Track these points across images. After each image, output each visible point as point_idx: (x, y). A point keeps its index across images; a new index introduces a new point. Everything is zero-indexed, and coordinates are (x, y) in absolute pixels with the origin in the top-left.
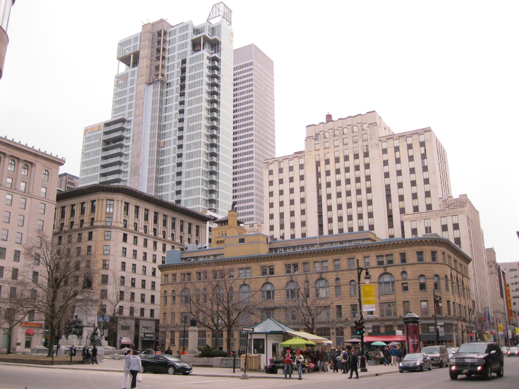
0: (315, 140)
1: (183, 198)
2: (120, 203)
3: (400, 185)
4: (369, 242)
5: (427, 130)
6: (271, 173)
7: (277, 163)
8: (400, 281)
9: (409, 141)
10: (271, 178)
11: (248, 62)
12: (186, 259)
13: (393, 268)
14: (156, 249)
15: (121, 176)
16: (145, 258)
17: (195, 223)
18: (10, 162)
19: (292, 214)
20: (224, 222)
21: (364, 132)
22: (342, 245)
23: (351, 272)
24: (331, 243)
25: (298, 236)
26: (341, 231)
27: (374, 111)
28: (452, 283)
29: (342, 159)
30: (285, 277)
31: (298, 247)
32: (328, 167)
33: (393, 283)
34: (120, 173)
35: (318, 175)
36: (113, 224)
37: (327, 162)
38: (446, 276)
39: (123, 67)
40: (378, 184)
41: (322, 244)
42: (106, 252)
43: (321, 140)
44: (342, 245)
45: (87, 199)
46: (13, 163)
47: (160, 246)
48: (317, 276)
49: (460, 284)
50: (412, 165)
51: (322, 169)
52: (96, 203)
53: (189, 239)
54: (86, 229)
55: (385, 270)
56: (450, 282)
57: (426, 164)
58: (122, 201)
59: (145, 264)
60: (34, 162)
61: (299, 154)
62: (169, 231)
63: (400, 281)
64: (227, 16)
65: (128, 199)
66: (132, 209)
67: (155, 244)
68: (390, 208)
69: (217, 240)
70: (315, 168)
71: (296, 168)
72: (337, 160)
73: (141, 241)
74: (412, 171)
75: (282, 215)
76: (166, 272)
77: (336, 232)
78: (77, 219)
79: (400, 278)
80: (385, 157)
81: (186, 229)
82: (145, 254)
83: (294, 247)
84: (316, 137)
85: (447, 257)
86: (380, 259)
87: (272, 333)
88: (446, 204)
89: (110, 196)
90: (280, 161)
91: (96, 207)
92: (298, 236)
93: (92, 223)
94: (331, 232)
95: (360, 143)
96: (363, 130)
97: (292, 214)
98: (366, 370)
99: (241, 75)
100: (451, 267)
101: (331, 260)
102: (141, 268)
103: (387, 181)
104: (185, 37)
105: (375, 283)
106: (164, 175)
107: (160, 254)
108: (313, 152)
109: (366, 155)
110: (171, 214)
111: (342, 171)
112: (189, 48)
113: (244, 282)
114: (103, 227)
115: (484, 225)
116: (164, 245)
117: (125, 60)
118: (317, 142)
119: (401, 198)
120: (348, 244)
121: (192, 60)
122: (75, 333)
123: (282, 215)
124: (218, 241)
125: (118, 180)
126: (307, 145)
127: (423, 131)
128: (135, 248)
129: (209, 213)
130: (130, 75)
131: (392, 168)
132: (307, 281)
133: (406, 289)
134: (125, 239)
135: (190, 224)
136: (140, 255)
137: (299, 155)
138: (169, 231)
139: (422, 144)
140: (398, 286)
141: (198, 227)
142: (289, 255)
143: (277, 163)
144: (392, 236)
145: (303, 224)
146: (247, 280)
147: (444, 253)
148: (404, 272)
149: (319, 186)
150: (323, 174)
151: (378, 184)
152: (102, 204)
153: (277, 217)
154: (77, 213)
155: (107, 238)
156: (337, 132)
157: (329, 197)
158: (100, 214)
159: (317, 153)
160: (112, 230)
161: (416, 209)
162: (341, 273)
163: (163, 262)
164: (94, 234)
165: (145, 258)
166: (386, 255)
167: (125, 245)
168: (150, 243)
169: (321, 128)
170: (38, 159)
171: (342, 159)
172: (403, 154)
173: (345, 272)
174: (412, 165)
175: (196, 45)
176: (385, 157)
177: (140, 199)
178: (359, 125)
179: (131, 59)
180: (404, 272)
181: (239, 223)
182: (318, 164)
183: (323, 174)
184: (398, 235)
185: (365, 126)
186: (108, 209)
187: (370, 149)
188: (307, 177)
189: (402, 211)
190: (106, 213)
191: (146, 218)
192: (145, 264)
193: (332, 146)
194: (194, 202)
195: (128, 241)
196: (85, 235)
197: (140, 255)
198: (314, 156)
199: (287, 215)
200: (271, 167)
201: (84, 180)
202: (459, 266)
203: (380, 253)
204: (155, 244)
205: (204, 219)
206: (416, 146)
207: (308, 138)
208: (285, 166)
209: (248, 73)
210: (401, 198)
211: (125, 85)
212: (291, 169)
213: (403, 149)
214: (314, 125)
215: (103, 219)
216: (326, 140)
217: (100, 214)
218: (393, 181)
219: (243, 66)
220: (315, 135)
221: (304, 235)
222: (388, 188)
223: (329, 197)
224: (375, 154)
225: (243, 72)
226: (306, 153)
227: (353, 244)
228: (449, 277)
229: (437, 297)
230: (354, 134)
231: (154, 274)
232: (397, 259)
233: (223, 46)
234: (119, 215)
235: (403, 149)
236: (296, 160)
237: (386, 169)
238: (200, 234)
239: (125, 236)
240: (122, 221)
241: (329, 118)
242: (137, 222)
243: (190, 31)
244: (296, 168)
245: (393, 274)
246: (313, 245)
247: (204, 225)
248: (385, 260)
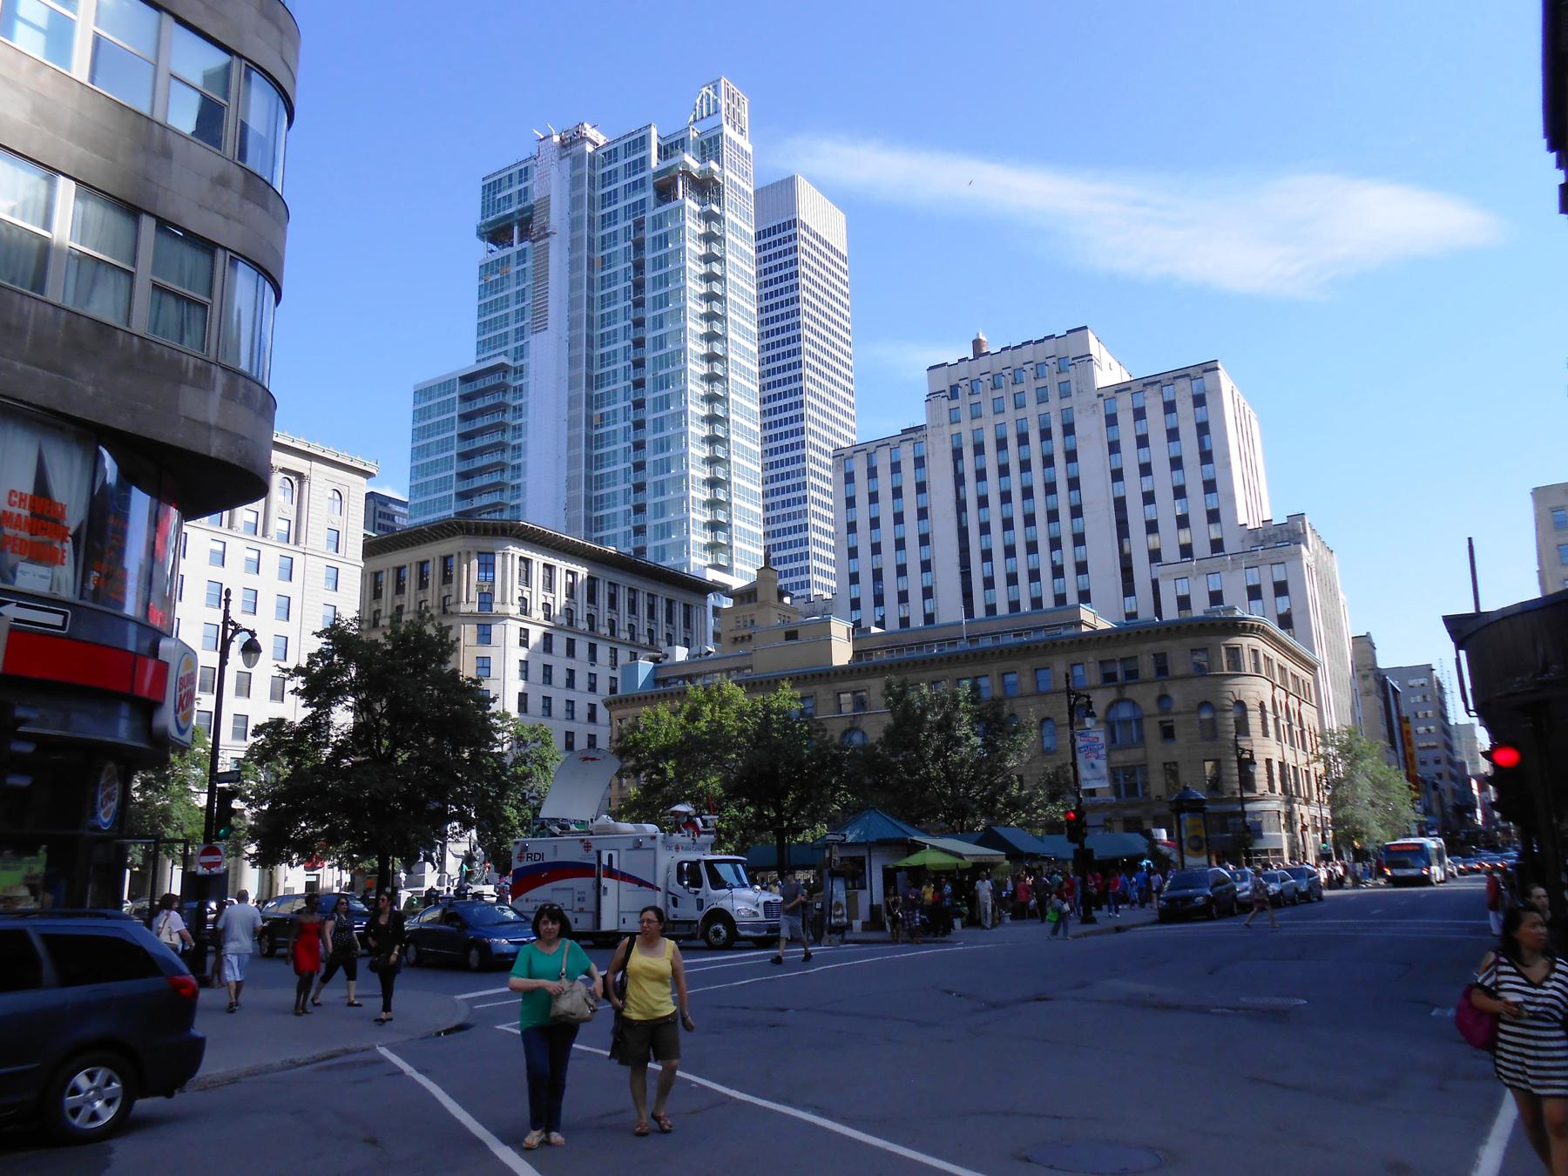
1: (651, 543)
3: (1149, 498)
4: (1084, 629)
7: (862, 456)
12: (664, 681)
13: (1139, 687)
15: (506, 497)
16: (570, 683)
17: (680, 598)
19: (902, 570)
20: (746, 596)
22: (1018, 639)
24: (995, 635)
25: (917, 622)
26: (1014, 606)
27: (1085, 328)
28: (1276, 720)
31: (920, 646)
33: (1139, 722)
35: (959, 480)
37: (979, 449)
38: (1262, 705)
40: (1097, 494)
41: (972, 639)
43: (964, 402)
44: (1018, 639)
45: (432, 552)
47: (603, 652)
49: (1295, 721)
51: (969, 464)
52: (455, 559)
53: (669, 636)
55: (1120, 693)
59: (571, 695)
60: (306, 473)
62: (624, 620)
66: (538, 573)
67: (592, 649)
68: (1126, 549)
69: (733, 634)
70: (951, 464)
71: (908, 466)
74: (1176, 463)
75: (878, 575)
76: (619, 713)
77: (1002, 609)
79: (1156, 710)
81: (661, 614)
82: (571, 672)
83: (910, 647)
84: (954, 392)
86: (1109, 669)
87: (883, 843)
88: (1256, 538)
90: (868, 450)
92: (917, 622)
94: (991, 609)
97: (902, 570)
98: (1093, 921)
101: (995, 673)
102: (563, 706)
106: (605, 491)
107: (603, 671)
108: (946, 428)
109: (1069, 429)
110: (624, 581)
112: (650, 194)
116: (614, 651)
118: (954, 404)
119: (1152, 527)
120: (1033, 637)
122: (429, 858)
123: (878, 575)
124: (736, 639)
125: (498, 507)
126: (930, 413)
127: (1200, 370)
129: (712, 575)
133: (1168, 733)
135: (670, 602)
136: (559, 676)
138: (624, 620)
140: (1152, 729)
141: (687, 607)
144: (1131, 616)
145: (928, 593)
148: (1163, 698)
149: (961, 506)
150: (970, 476)
153: (866, 578)
154: (411, 583)
157: (985, 529)
161: (1186, 550)
162: (1020, 701)
163: (613, 690)
165: (570, 683)
166: (1122, 660)
168: (582, 648)
169: (963, 370)
171: (1012, 443)
172: (1156, 424)
173: (1029, 701)
180: (1163, 698)
181: (781, 594)
182: (957, 454)
183: (970, 476)
184: (1146, 613)
189: (1155, 556)
192: (571, 695)
197: (559, 676)
198: (948, 438)
199: (889, 574)
201: (423, 508)
203: (1108, 654)
204: (592, 649)
205: (702, 588)
207: (932, 396)
208: (883, 461)
209: (786, 246)
210: (1152, 527)
212: (896, 467)
216: (975, 399)
218: (1132, 488)
220: (950, 389)
221: (929, 618)
222: (1120, 504)
226: (929, 432)
227: (1043, 635)
229: (1243, 751)
231: (592, 717)
232: (1147, 668)
238: (694, 624)
239: (525, 633)
241: (977, 344)
242: (550, 601)
244: (908, 466)
246: (953, 641)
247: (701, 601)
248: (1119, 670)
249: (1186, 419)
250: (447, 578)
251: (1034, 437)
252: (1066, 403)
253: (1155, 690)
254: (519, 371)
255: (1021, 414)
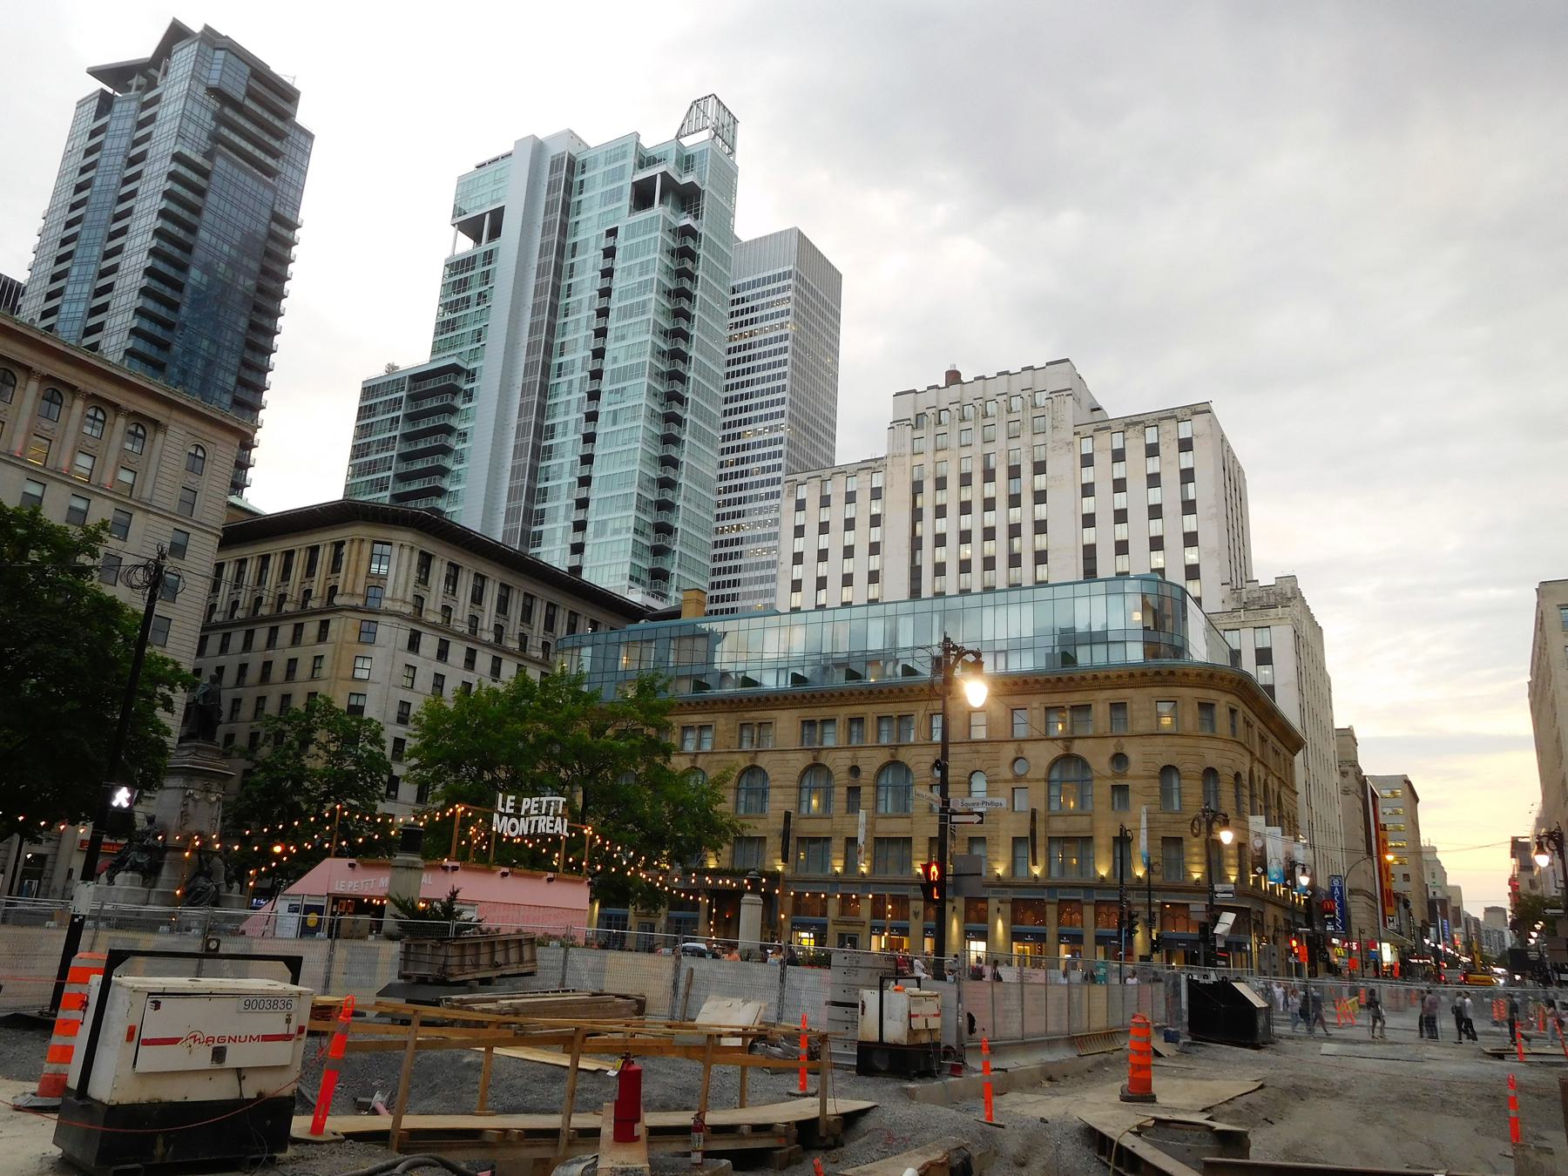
0: (916, 427)
2: (406, 551)
5: (1200, 408)
6: (800, 506)
7: (817, 482)
8: (1107, 778)
9: (1151, 436)
10: (800, 519)
11: (781, 270)
14: (498, 676)
15: (441, 504)
18: (91, 412)
21: (1037, 413)
23: (973, 747)
28: (1252, 796)
29: (977, 478)
30: (799, 755)
32: (942, 497)
34: (439, 496)
35: (917, 515)
36: (386, 604)
37: (941, 484)
38: (1237, 776)
39: (465, 245)
42: (358, 674)
43: (928, 432)
46: (140, 432)
48: (882, 757)
49: (1273, 802)
50: (1155, 496)
51: (927, 502)
52: (345, 549)
54: (315, 612)
55: (1067, 748)
56: (1246, 792)
57: (1191, 497)
58: (412, 548)
60: (163, 420)
61: (871, 466)
63: (1107, 778)
64: (725, 130)
65: (429, 546)
66: (439, 570)
70: (908, 497)
71: (863, 497)
72: (965, 480)
73: (457, 651)
78: (294, 588)
79: (1108, 772)
80: (1088, 475)
84: (918, 421)
85: (1240, 723)
88: (1239, 599)
89: (380, 533)
91: (345, 558)
93: (330, 599)
95: (1026, 437)
96: (1035, 406)
99: (763, 301)
100: (1252, 753)
103: (1089, 536)
104: (619, 174)
105: (1038, 780)
108: (908, 458)
109: (1040, 468)
110: (544, 596)
111: (977, 506)
112: (626, 201)
113: (693, 761)
114: (355, 609)
115: (1335, 660)
117: (471, 227)
118: (918, 434)
121: (632, 231)
122: (134, 868)
126: (893, 442)
128: (441, 668)
130: (479, 262)
131: (1104, 503)
132: (855, 770)
134: (414, 644)
137: (872, 464)
139: (1186, 445)
140: (1101, 791)
142: (813, 696)
143: (817, 482)
146: (700, 758)
147: (1233, 711)
148: (1119, 759)
149: (916, 543)
150: (928, 513)
151: (1065, 544)
152: (359, 553)
154: (298, 571)
155: (367, 635)
156: (969, 411)
157: (940, 569)
158: (351, 576)
159: (918, 460)
160: (381, 619)
164: (333, 626)
167: (412, 659)
170: (175, 415)
171: (977, 478)
174: (1155, 496)
175: (642, 196)
176: (1088, 475)
177: (462, 546)
178: (1025, 394)
179: (481, 226)
180: (1119, 759)
182: (917, 488)
183: (928, 513)
185: (1041, 399)
186: (375, 567)
187: (1050, 453)
188: (887, 521)
190: (369, 575)
191: (477, 598)
193: (954, 444)
194: (610, 569)
195: (421, 650)
196: (311, 628)
200: (803, 493)
202: (1271, 753)
205: (632, 613)
206: (1169, 450)
208: (836, 489)
211: (462, 285)
212: (850, 498)
213: (1135, 452)
214: (914, 391)
215: (360, 590)
216: (941, 430)
217: (351, 576)
218: (1104, 535)
219: (769, 280)
220: (916, 418)
222: (1090, 552)
223: (940, 569)
224: (1063, 474)
225: (768, 293)
226: (889, 461)
228: (1245, 776)
230: (1013, 417)
233: (706, 203)
234: (402, 580)
235: (1135, 452)
236: (863, 476)
237: (1088, 505)
240: (409, 598)
241: (953, 377)
243: (631, 161)
244: (863, 497)
245: (1088, 759)
249: (1170, 463)
250: (336, 566)
251: (1001, 474)
252: (1039, 440)
253: (1110, 747)
254: (471, 375)
255: (989, 448)
